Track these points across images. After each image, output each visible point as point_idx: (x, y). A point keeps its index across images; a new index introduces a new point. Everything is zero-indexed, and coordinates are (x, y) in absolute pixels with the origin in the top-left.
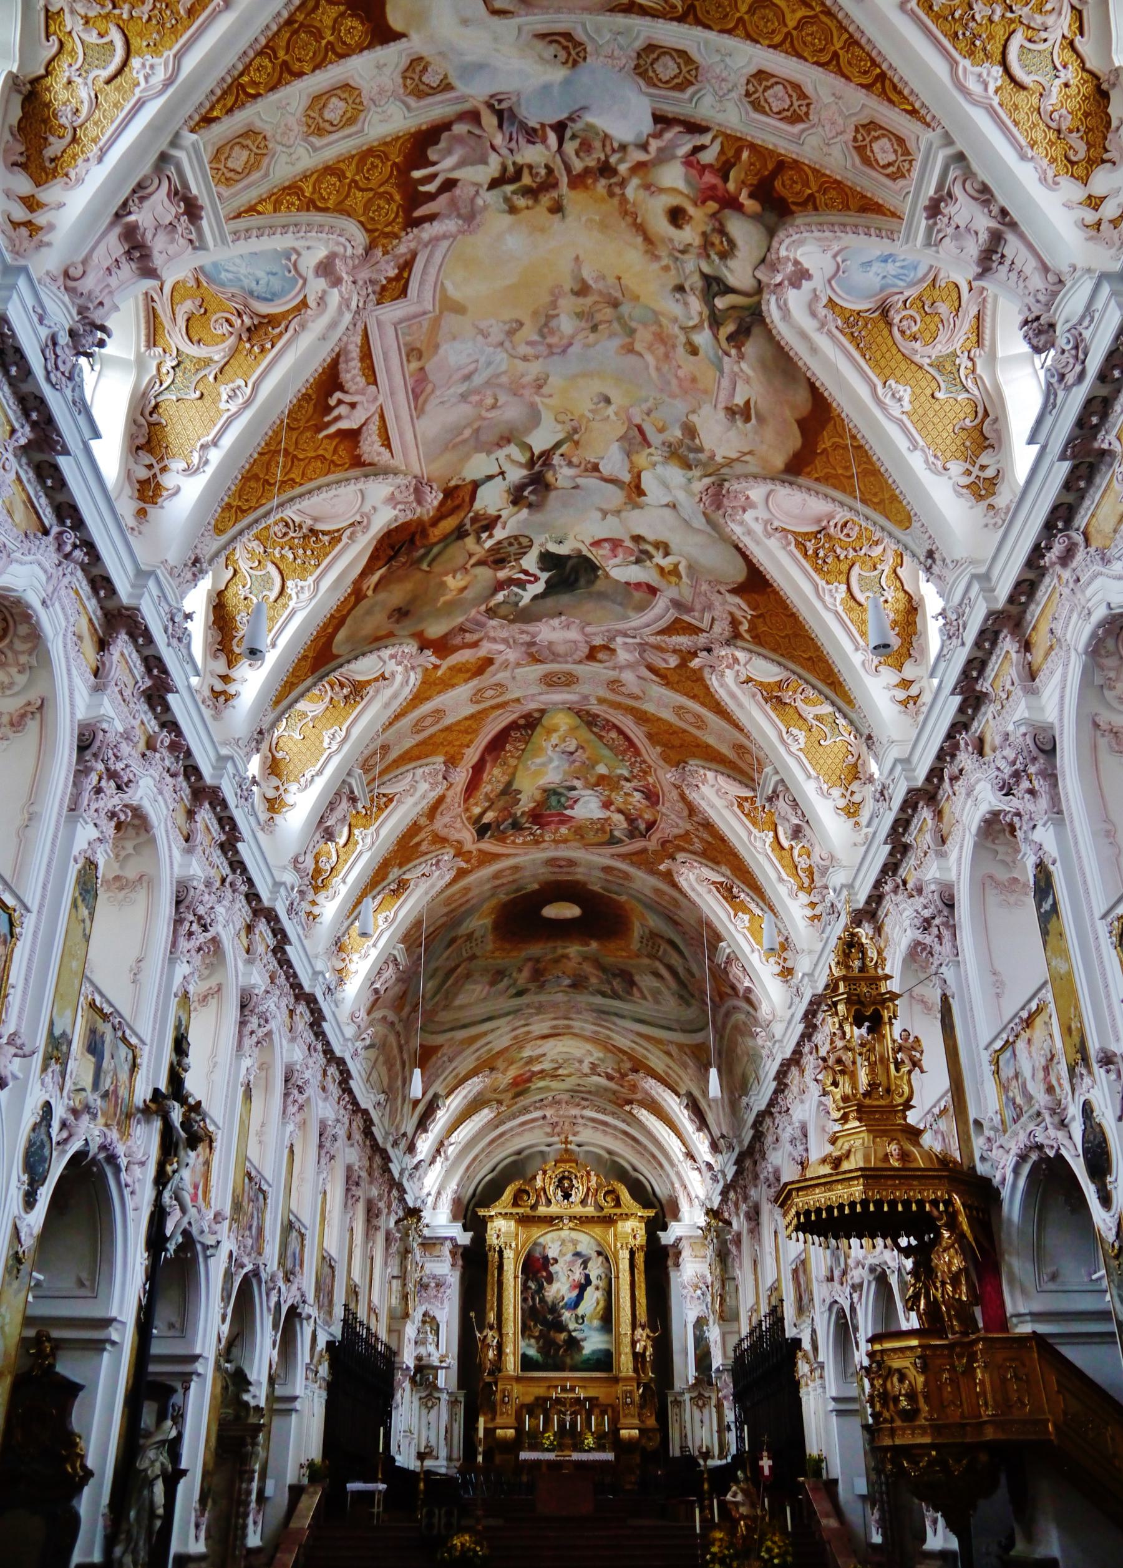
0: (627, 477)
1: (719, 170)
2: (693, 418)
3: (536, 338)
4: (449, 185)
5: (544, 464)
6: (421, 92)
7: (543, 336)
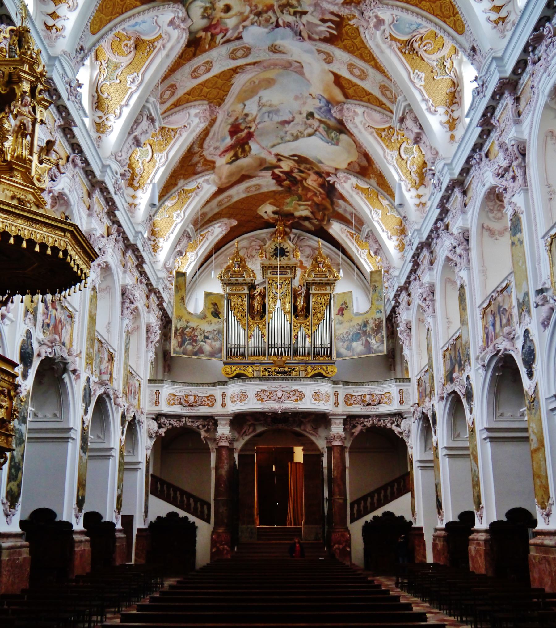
1: (215, 35)
4: (324, 21)
6: (328, 54)
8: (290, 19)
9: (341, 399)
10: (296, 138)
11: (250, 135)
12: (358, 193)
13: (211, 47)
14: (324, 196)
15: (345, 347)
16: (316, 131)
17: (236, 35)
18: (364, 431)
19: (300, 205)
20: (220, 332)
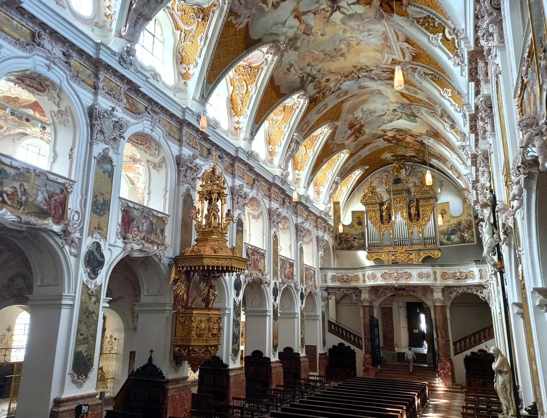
0: (303, 18)
2: (297, 53)
3: (351, 42)
4: (384, 72)
5: (334, 7)
7: (348, 42)
8: (365, 74)
9: (438, 276)
10: (391, 121)
11: (362, 126)
12: (439, 144)
13: (324, 98)
14: (420, 146)
15: (446, 238)
16: (401, 117)
17: (337, 88)
18: (459, 295)
19: (407, 151)
20: (363, 234)
